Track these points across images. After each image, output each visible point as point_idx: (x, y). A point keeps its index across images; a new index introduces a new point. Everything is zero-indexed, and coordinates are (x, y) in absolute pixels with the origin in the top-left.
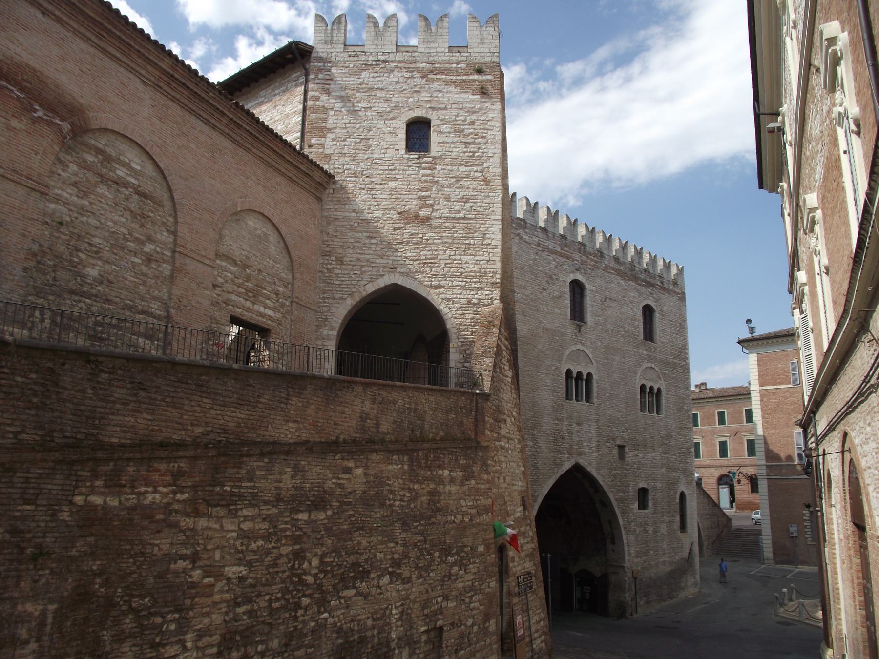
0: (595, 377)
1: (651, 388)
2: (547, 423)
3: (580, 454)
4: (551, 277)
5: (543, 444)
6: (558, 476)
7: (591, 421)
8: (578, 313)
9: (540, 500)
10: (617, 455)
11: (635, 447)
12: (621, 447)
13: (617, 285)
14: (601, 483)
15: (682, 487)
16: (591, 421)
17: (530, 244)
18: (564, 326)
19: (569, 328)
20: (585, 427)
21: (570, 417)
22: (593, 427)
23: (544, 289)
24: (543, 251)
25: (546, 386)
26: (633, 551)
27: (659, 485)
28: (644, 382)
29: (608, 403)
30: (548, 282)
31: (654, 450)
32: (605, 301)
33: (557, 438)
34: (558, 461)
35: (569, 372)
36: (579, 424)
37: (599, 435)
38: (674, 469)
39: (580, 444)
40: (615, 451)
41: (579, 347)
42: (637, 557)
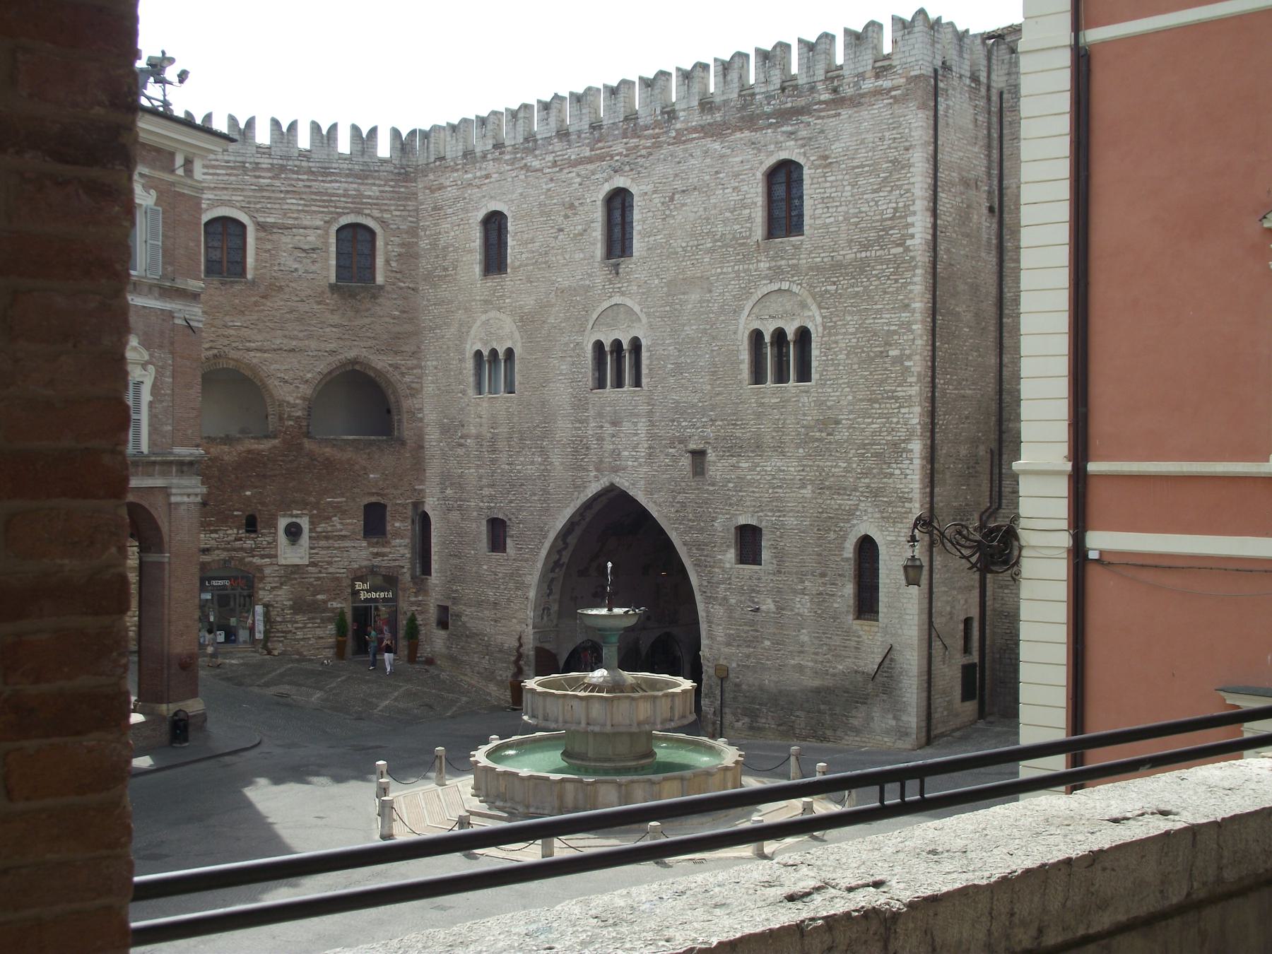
0: (644, 342)
1: (780, 335)
2: (564, 429)
3: (615, 470)
4: (572, 206)
5: (556, 460)
6: (579, 503)
7: (637, 415)
8: (618, 241)
9: (552, 536)
10: (689, 468)
11: (733, 449)
12: (699, 455)
13: (700, 158)
14: (655, 515)
15: (866, 526)
16: (637, 415)
17: (541, 170)
18: (590, 275)
19: (600, 275)
20: (627, 427)
21: (600, 415)
22: (642, 427)
23: (561, 230)
24: (561, 170)
25: (561, 374)
26: (720, 633)
27: (791, 521)
29: (672, 380)
30: (566, 217)
31: (783, 454)
32: (672, 199)
33: (579, 448)
34: (579, 482)
35: (599, 346)
36: (614, 424)
37: (652, 436)
38: (840, 490)
39: (616, 454)
40: (686, 461)
41: (617, 299)
42: (728, 644)
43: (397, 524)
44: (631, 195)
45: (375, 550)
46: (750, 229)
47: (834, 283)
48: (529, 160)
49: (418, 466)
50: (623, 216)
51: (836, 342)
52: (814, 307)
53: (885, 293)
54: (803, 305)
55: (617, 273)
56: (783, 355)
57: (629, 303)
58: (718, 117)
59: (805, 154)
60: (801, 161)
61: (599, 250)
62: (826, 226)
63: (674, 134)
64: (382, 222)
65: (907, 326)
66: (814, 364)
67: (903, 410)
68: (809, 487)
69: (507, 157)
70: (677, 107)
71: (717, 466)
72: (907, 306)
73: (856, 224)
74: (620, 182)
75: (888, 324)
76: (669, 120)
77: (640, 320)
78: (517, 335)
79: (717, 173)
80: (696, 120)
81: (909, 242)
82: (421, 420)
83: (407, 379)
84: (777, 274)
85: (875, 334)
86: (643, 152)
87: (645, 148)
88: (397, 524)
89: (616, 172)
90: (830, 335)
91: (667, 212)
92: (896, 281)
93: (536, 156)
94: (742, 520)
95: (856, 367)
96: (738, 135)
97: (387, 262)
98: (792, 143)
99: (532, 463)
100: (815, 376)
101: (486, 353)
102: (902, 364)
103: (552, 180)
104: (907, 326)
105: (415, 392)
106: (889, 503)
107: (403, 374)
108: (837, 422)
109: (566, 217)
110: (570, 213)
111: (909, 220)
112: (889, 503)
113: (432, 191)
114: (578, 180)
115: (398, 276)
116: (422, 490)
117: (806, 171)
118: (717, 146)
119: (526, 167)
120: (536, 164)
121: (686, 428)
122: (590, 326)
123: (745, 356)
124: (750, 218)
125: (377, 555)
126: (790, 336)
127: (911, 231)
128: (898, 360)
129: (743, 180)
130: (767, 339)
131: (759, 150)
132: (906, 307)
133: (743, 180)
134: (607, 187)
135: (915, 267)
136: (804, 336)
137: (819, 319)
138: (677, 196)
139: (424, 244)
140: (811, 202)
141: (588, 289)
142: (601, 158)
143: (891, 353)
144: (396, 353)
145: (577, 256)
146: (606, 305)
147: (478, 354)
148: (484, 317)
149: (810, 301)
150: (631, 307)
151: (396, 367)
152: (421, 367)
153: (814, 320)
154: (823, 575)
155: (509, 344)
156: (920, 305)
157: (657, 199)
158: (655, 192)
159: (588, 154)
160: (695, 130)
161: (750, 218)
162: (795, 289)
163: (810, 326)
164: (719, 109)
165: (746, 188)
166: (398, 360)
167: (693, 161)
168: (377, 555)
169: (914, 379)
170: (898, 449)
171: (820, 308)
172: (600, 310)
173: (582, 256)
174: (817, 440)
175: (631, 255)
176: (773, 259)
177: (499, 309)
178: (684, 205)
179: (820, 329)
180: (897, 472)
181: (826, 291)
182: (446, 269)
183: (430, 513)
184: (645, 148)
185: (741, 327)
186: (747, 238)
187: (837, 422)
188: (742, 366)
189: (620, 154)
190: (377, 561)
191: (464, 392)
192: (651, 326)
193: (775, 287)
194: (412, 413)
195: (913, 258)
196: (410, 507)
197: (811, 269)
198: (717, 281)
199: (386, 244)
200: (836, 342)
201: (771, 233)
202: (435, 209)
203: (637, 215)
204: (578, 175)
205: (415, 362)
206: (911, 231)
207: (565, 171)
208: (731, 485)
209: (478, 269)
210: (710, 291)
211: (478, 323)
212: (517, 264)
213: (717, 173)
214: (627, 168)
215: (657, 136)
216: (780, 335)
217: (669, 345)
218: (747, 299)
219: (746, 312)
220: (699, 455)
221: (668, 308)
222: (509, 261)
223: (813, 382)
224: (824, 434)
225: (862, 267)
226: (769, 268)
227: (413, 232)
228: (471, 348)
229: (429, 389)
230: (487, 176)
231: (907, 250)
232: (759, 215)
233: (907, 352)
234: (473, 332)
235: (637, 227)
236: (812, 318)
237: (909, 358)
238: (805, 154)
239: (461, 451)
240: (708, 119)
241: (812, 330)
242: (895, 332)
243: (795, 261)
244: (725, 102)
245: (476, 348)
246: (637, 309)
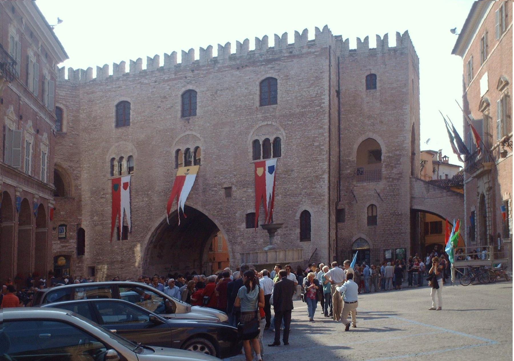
0: (202, 148)
17: (149, 84)
28: (256, 138)
29: (215, 162)
32: (216, 93)
43: (71, 233)
44: (196, 92)
45: (63, 245)
46: (253, 103)
47: (291, 121)
49: (79, 208)
50: (190, 100)
51: (292, 142)
52: (282, 130)
53: (313, 123)
54: (277, 129)
55: (188, 123)
56: (268, 148)
57: (194, 133)
58: (238, 62)
59: (278, 75)
60: (277, 77)
61: (179, 114)
62: (287, 101)
63: (217, 69)
64: (66, 106)
65: (322, 134)
66: (282, 150)
67: (320, 164)
68: (280, 196)
69: (131, 79)
70: (218, 59)
71: (237, 193)
72: (322, 127)
73: (300, 99)
74: (190, 87)
75: (314, 134)
76: (215, 64)
77: (200, 140)
78: (135, 150)
79: (237, 83)
80: (228, 63)
81: (322, 105)
82: (80, 189)
83: (75, 172)
84: (265, 119)
85: (308, 138)
86: (202, 76)
87: (202, 74)
88: (71, 233)
89: (188, 83)
90: (289, 139)
91: (214, 98)
92: (317, 119)
93: (146, 79)
95: (300, 150)
96: (247, 69)
97: (68, 123)
98: (272, 71)
99: (143, 201)
100: (282, 154)
101: (117, 158)
102: (320, 148)
103: (154, 87)
104: (322, 134)
105: (77, 178)
106: (315, 198)
107: (74, 170)
108: (292, 171)
109: (162, 102)
110: (164, 100)
111: (322, 97)
112: (315, 198)
113: (88, 94)
114: (169, 87)
115: (72, 129)
116: (81, 219)
117: (278, 81)
118: (238, 73)
119: (141, 83)
120: (146, 81)
122: (174, 144)
123: (251, 150)
124: (253, 98)
125: (63, 247)
126: (272, 141)
127: (323, 101)
128: (318, 147)
129: (250, 85)
130: (261, 143)
131: (258, 74)
132: (321, 128)
133: (250, 85)
134: (184, 89)
135: (325, 113)
136: (277, 141)
137: (284, 134)
138: (218, 92)
139: (82, 116)
140: (281, 92)
142: (181, 78)
143: (315, 144)
144: (71, 161)
145: (167, 117)
147: (113, 159)
148: (117, 144)
149: (280, 127)
150: (196, 134)
151: (71, 167)
152: (80, 167)
153: (282, 135)
155: (131, 154)
156: (326, 127)
157: (209, 94)
158: (208, 90)
159: (173, 76)
160: (227, 67)
161: (253, 98)
162: (274, 123)
163: (281, 137)
164: (238, 59)
165: (251, 88)
166: (72, 164)
167: (227, 79)
168: (63, 247)
169: (325, 153)
170: (318, 178)
171: (285, 130)
172: (179, 137)
173: (170, 116)
174: (283, 178)
175: (195, 115)
176: (263, 113)
177: (125, 140)
179: (285, 138)
180: (319, 186)
181: (287, 124)
182: (95, 126)
184: (202, 74)
185: (249, 139)
186: (251, 106)
187: (292, 171)
189: (191, 77)
190: (64, 249)
191: (105, 176)
192: (205, 141)
193: (265, 123)
194: (76, 186)
195: (324, 110)
196: (75, 228)
197: (281, 116)
198: (238, 122)
199: (68, 116)
200: (292, 142)
201: (261, 105)
202: (89, 101)
203: (198, 100)
204: (168, 85)
205: (78, 165)
206: (323, 101)
207: (161, 84)
209: (114, 125)
210: (234, 127)
212: (136, 122)
213: (237, 83)
214: (194, 82)
215: (209, 69)
216: (267, 141)
217: (214, 148)
218: (252, 129)
219: (251, 134)
221: (214, 134)
222: (131, 121)
223: (282, 157)
224: (287, 176)
225: (303, 114)
226: (262, 117)
227: (78, 111)
228: (108, 158)
229: (85, 175)
230: (119, 88)
231: (322, 107)
232: (257, 98)
233: (322, 143)
234: (110, 151)
235: (199, 104)
236: (282, 134)
237: (323, 145)
238: (278, 75)
239: (103, 200)
240: (234, 63)
241: (281, 138)
242: (316, 137)
243: (274, 114)
244: (241, 57)
245: (112, 157)
246: (198, 135)
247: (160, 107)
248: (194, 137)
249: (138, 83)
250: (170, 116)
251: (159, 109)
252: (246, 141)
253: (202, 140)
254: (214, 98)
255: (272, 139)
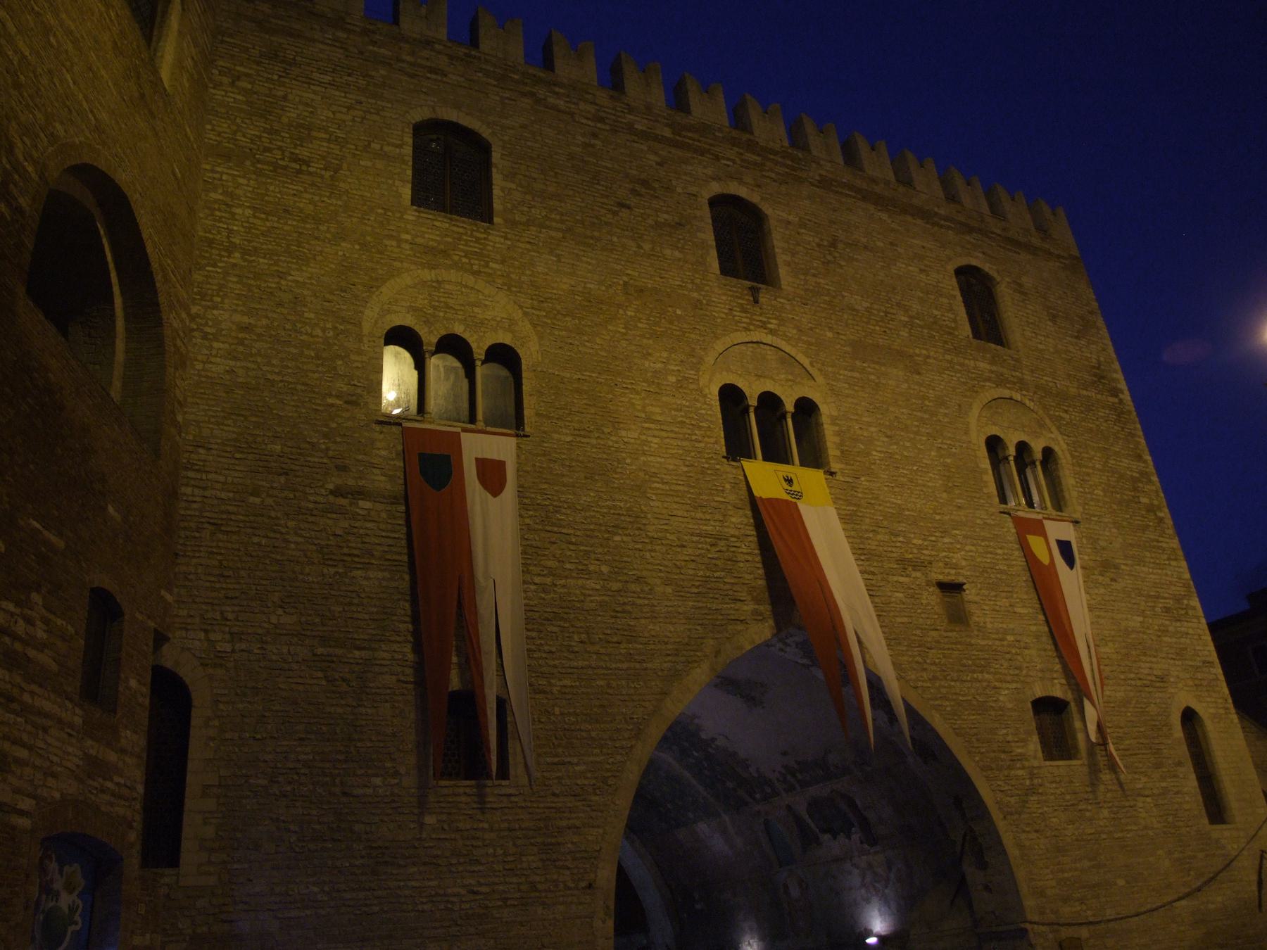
0: (826, 411)
28: (995, 431)
35: (731, 396)
40: (932, 598)
47: (1066, 412)
48: (541, 92)
55: (756, 301)
91: (829, 258)
94: (1039, 692)
118: (884, 216)
121: (920, 548)
141: (697, 305)
146: (742, 337)
148: (427, 275)
149: (1047, 421)
154: (1158, 766)
163: (1056, 448)
178: (857, 260)
183: (189, 672)
188: (985, 478)
193: (1007, 393)
208: (1010, 638)
210: (919, 373)
211: (407, 280)
220: (951, 588)
222: (497, 205)
247: (629, 208)
248: (788, 360)
249: (524, 95)
250: (677, 254)
251: (624, 213)
252: (967, 433)
253: (820, 380)
254: (829, 258)
255: (1037, 447)
